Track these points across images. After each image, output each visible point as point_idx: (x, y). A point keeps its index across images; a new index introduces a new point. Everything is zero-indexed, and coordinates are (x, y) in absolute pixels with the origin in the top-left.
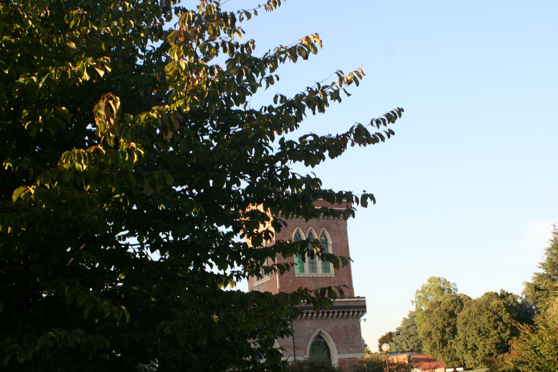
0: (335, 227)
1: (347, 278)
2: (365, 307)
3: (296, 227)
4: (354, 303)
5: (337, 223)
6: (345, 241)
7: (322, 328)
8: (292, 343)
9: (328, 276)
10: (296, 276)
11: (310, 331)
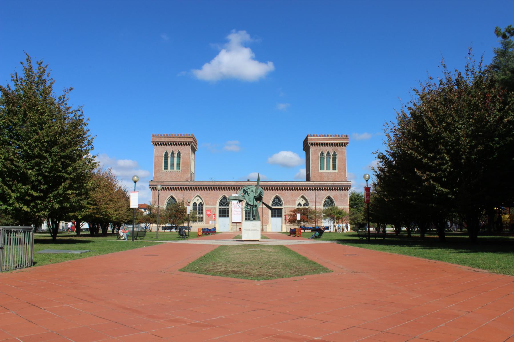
2: (350, 186)
9: (335, 172)
10: (319, 171)
11: (324, 195)
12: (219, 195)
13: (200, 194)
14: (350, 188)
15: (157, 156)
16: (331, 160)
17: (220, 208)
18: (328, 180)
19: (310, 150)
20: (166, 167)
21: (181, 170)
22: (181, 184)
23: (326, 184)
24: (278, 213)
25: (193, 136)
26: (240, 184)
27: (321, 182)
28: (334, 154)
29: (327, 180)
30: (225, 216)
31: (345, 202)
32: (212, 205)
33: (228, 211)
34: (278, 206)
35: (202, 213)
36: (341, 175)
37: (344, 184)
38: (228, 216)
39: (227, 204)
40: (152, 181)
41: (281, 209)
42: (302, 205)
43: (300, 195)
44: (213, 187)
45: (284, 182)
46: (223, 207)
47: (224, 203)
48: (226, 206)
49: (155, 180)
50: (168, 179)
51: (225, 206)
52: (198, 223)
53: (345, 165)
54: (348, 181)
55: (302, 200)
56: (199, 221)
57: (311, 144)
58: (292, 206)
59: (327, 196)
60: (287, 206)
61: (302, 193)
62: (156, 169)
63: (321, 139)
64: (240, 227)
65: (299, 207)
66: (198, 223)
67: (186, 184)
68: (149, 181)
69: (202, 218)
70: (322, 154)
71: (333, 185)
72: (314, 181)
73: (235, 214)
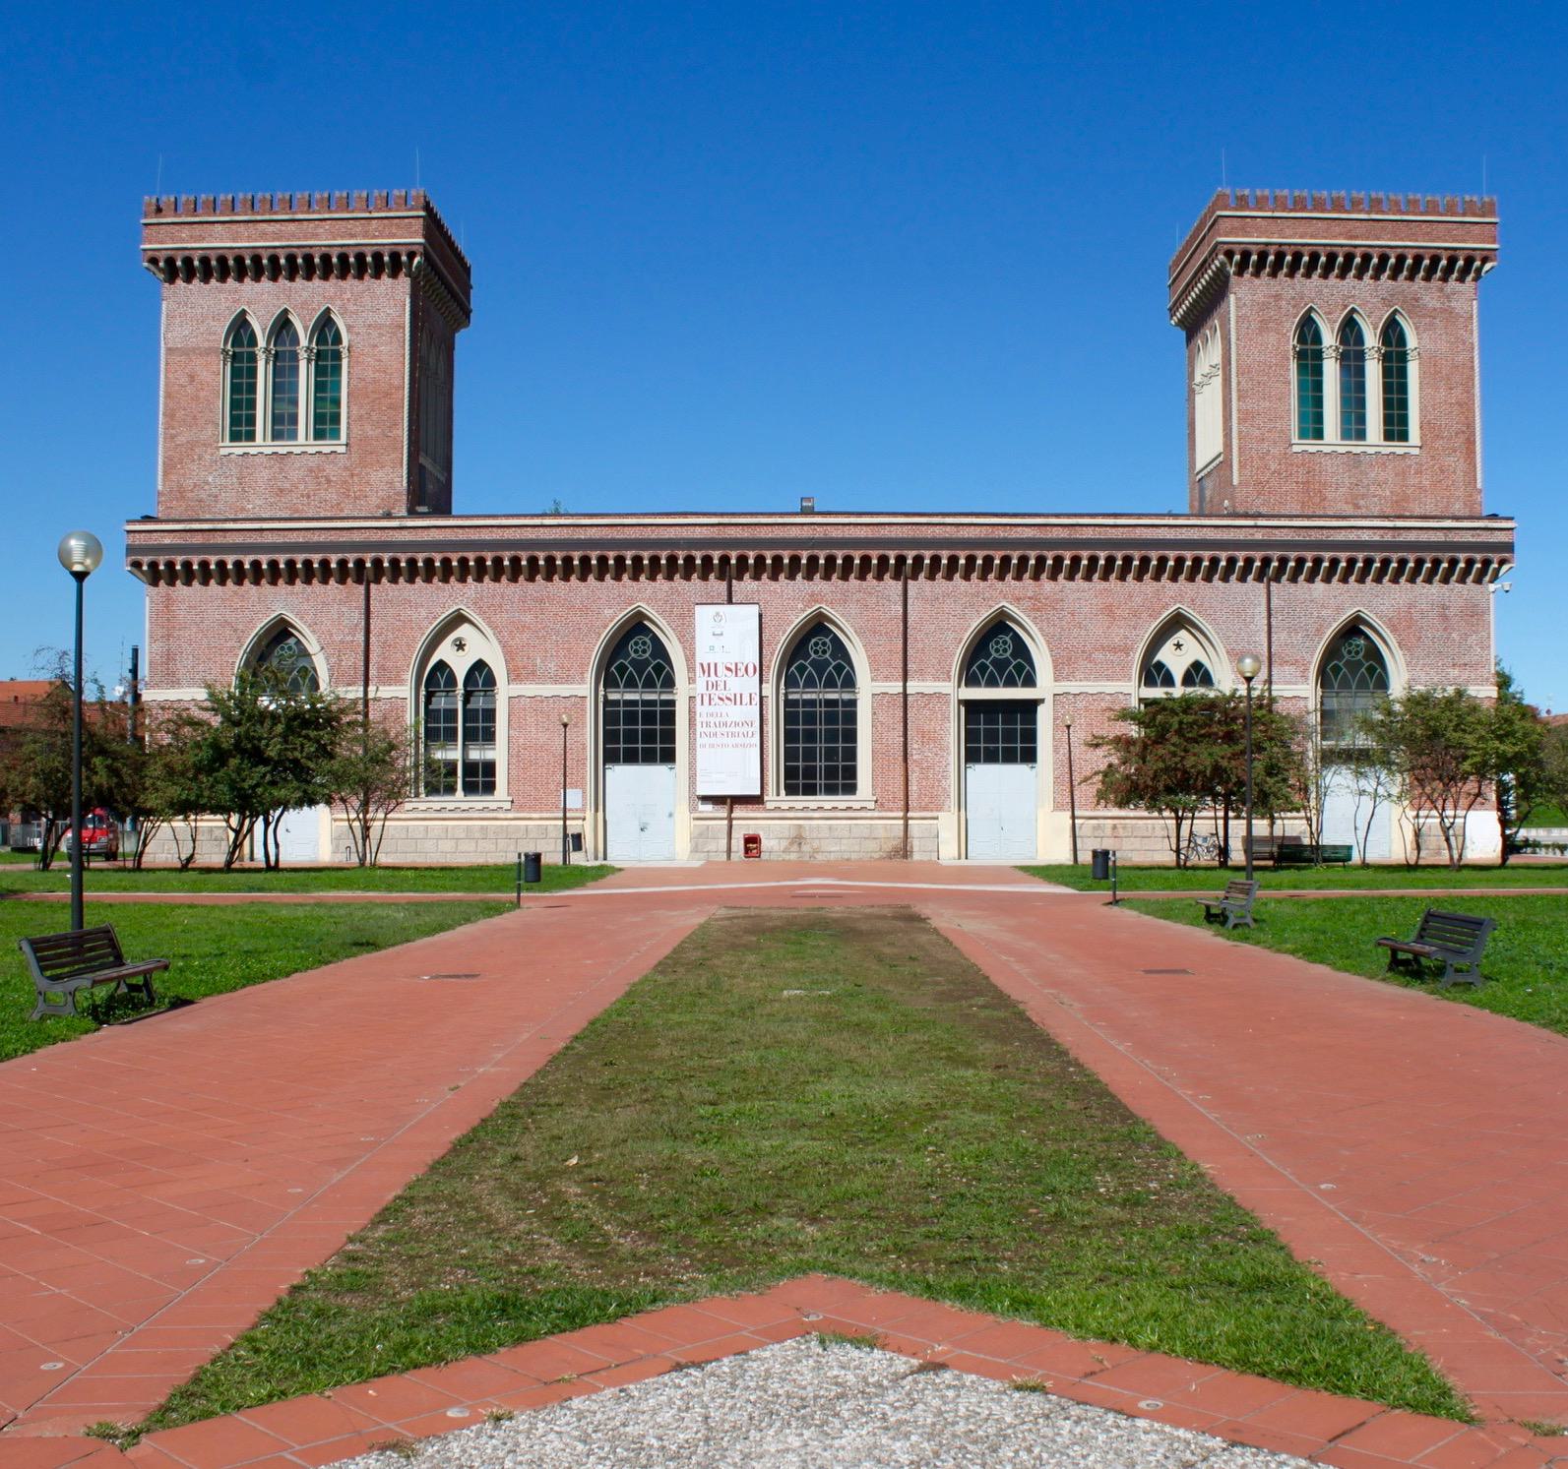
0: (1434, 302)
1: (1462, 460)
2: (1509, 547)
3: (1306, 305)
4: (1473, 536)
5: (1441, 290)
6: (1464, 344)
7: (1364, 605)
8: (1266, 645)
9: (1400, 451)
10: (1296, 449)
13: (476, 604)
14: (1502, 562)
15: (185, 352)
16: (1373, 372)
17: (612, 697)
18: (1357, 506)
19: (1232, 297)
20: (241, 427)
21: (343, 439)
22: (345, 537)
23: (1341, 536)
24: (1009, 736)
25: (427, 207)
26: (745, 533)
27: (1309, 517)
28: (1392, 333)
29: (1349, 510)
30: (649, 758)
31: (1466, 659)
32: (557, 680)
33: (669, 717)
34: (1010, 683)
35: (489, 736)
36: (1442, 471)
37: (1468, 537)
38: (669, 757)
39: (659, 669)
40: (147, 519)
41: (1030, 707)
42: (1178, 677)
43: (1166, 606)
44: (564, 554)
45: (1057, 516)
46: (629, 697)
47: (640, 666)
48: (654, 686)
49: (173, 516)
50: (256, 505)
51: (649, 684)
52: (464, 806)
53: (1466, 406)
54: (1494, 517)
55: (1178, 646)
56: (470, 788)
57: (1237, 257)
58: (1110, 687)
59: (1350, 612)
60: (1073, 687)
61: (1176, 595)
62: (173, 437)
63: (1301, 227)
64: (751, 832)
65: (1157, 692)
66: (422, 806)
67: (375, 537)
68: (129, 522)
69: (489, 768)
70: (1308, 330)
71: (1388, 537)
72: (1259, 516)
73: (713, 740)
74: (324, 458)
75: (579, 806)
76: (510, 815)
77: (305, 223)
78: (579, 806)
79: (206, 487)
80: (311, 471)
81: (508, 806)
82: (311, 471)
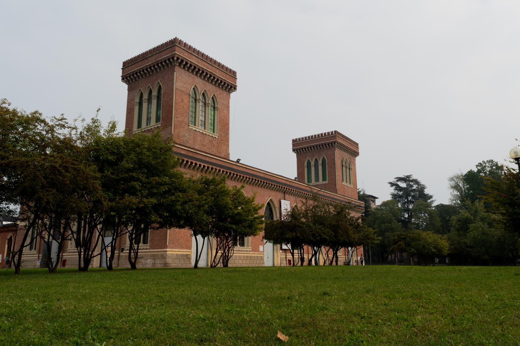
12: (267, 198)
52: (240, 249)
74: (213, 138)
75: (262, 251)
76: (252, 253)
77: (214, 67)
78: (262, 251)
79: (185, 137)
80: (210, 141)
81: (250, 250)
82: (210, 141)
